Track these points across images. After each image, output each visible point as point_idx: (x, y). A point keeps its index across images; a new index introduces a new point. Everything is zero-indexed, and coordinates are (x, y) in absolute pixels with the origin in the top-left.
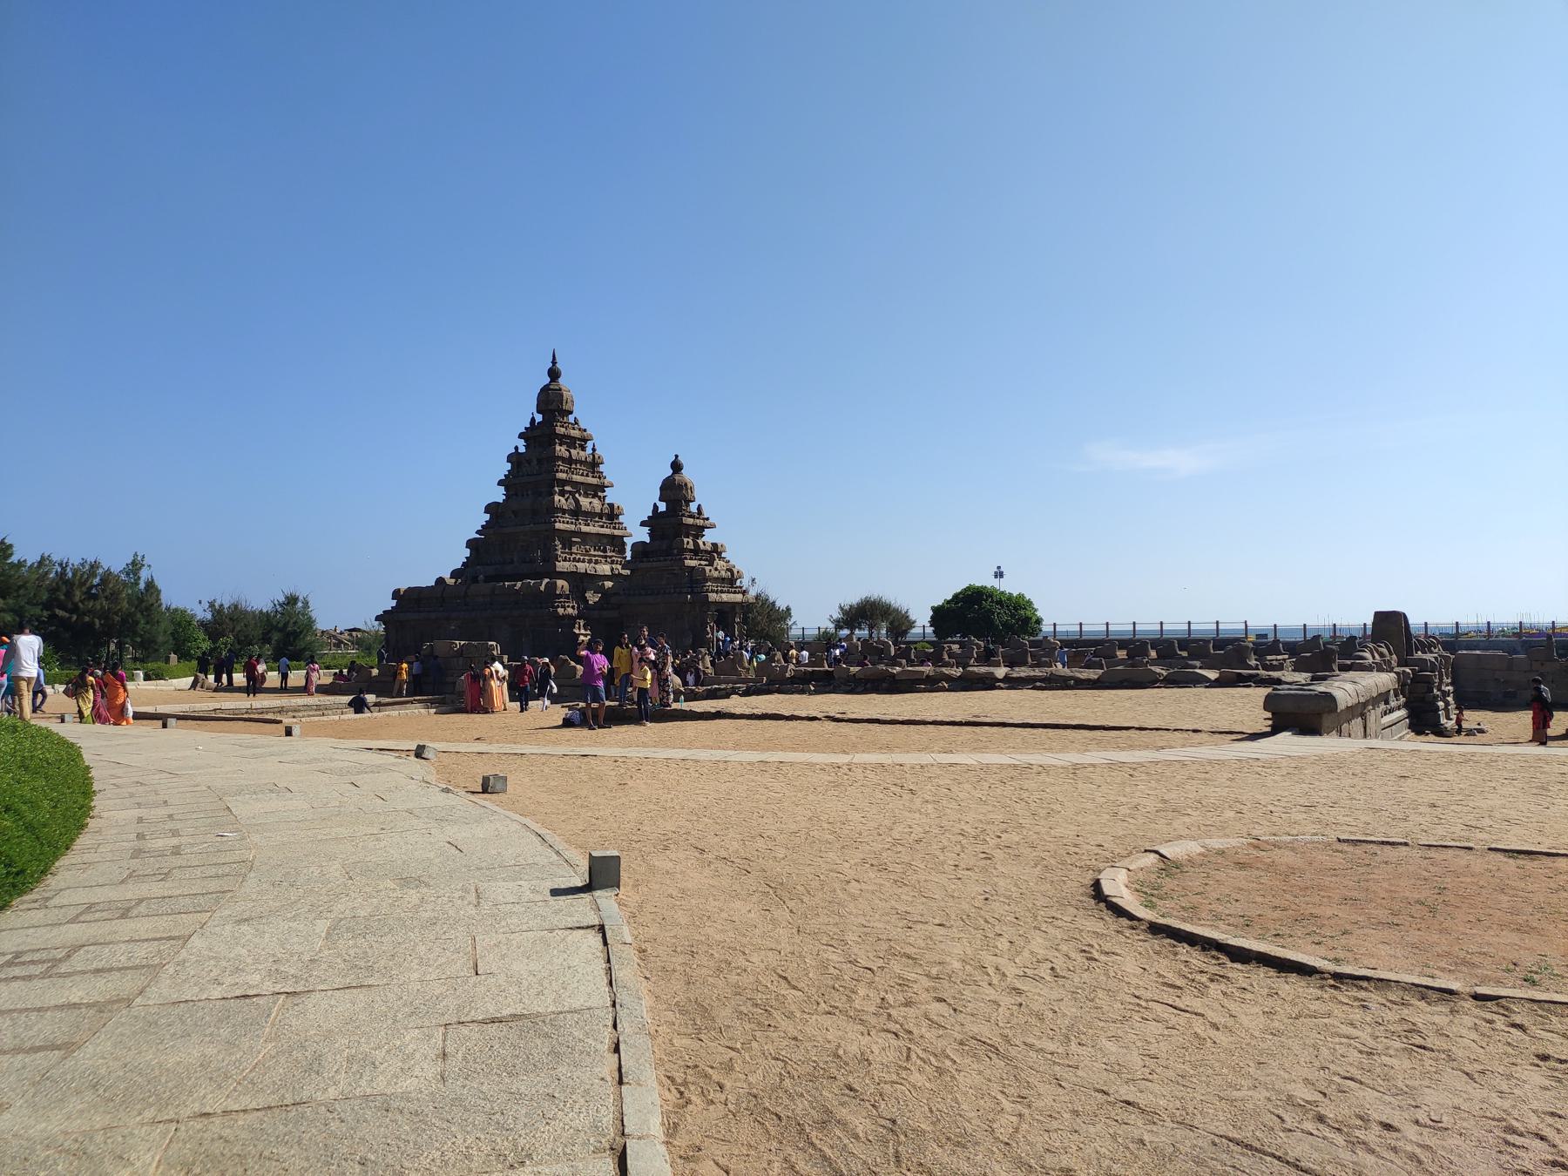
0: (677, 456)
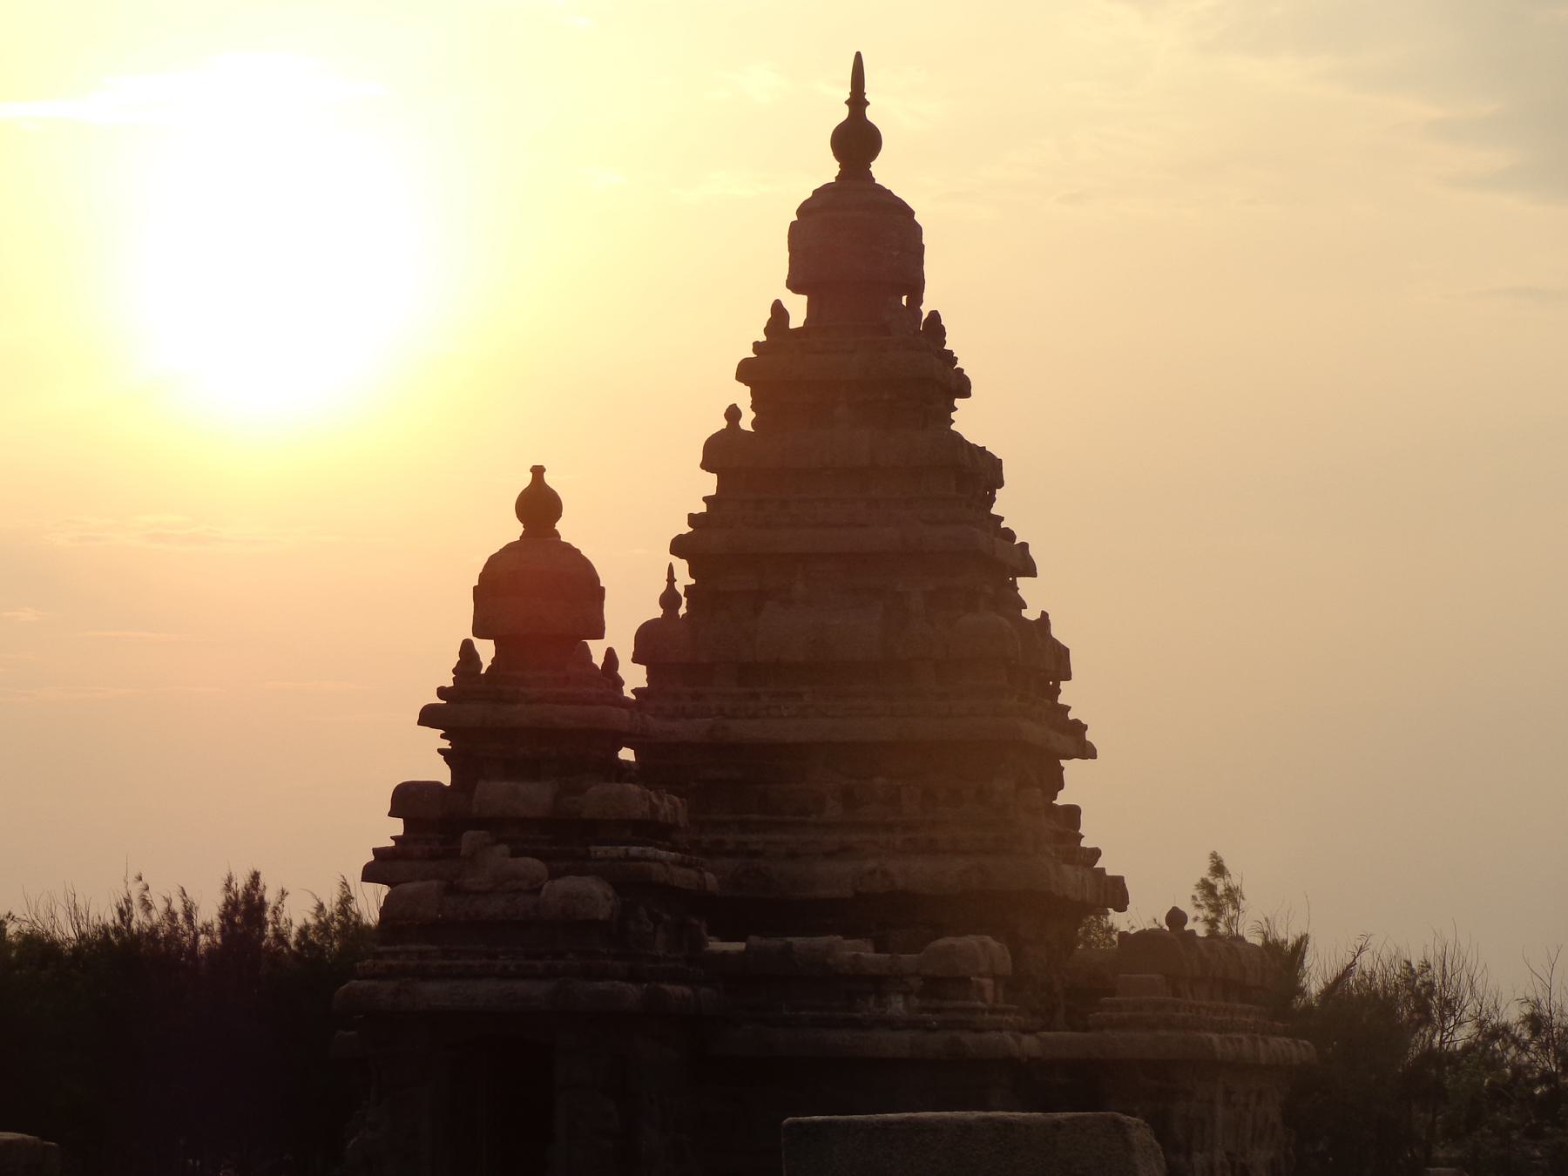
0: (538, 472)
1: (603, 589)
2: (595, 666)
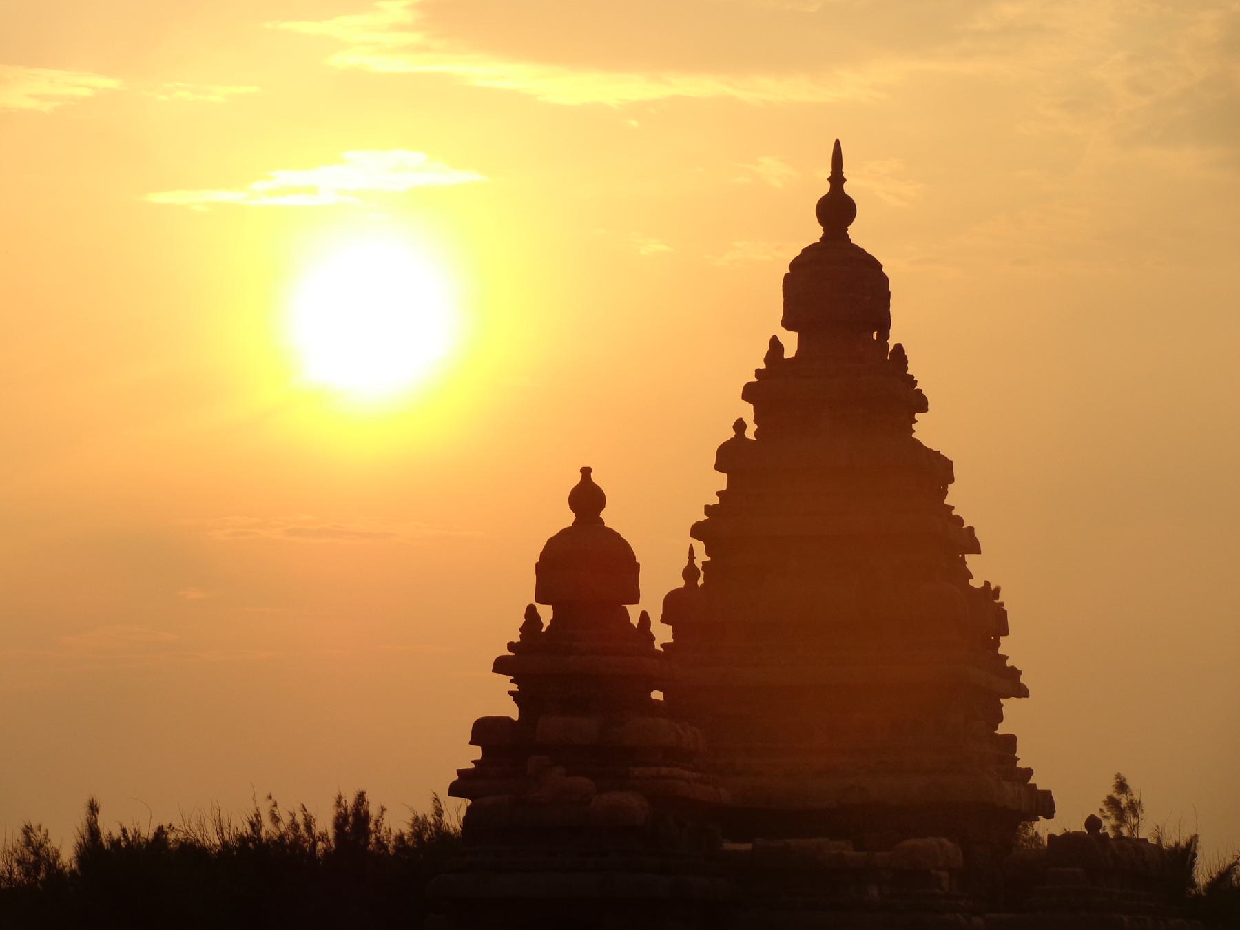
0: (586, 472)
1: (639, 564)
2: (633, 625)
